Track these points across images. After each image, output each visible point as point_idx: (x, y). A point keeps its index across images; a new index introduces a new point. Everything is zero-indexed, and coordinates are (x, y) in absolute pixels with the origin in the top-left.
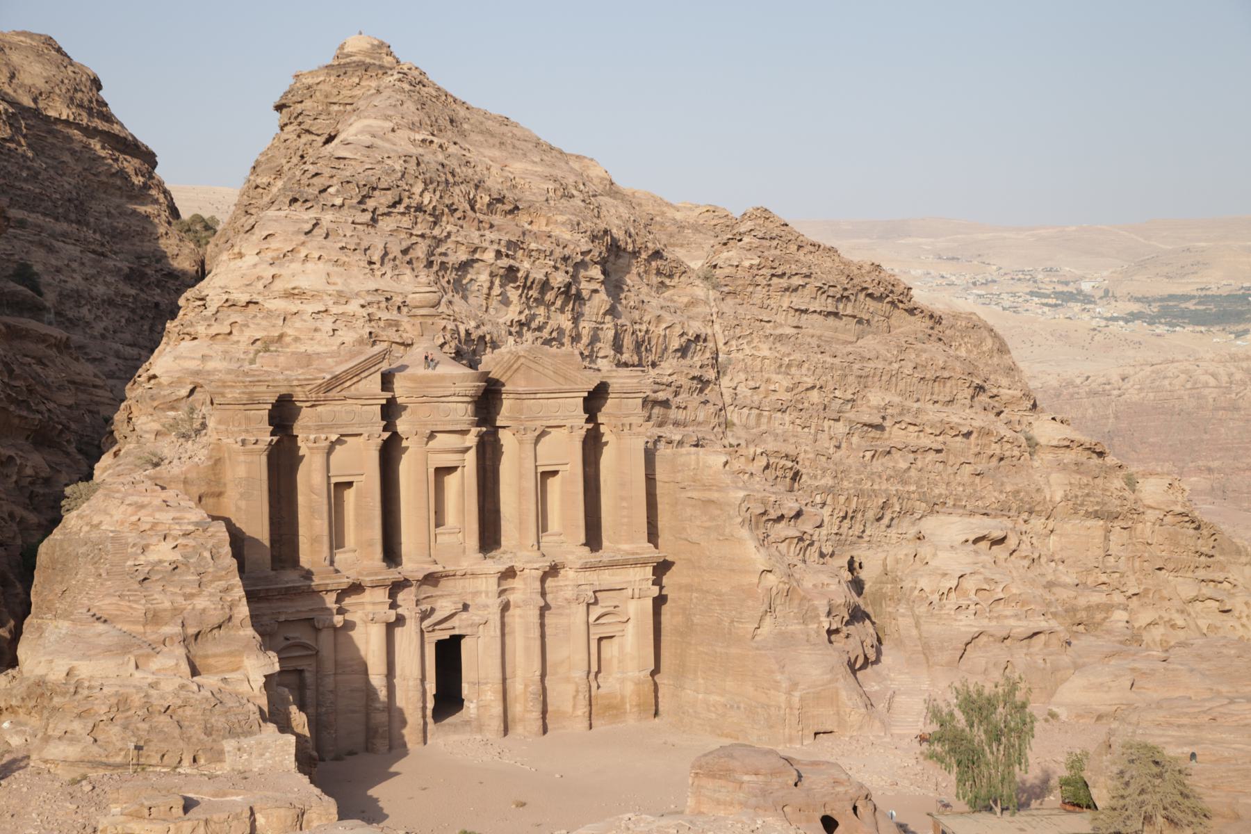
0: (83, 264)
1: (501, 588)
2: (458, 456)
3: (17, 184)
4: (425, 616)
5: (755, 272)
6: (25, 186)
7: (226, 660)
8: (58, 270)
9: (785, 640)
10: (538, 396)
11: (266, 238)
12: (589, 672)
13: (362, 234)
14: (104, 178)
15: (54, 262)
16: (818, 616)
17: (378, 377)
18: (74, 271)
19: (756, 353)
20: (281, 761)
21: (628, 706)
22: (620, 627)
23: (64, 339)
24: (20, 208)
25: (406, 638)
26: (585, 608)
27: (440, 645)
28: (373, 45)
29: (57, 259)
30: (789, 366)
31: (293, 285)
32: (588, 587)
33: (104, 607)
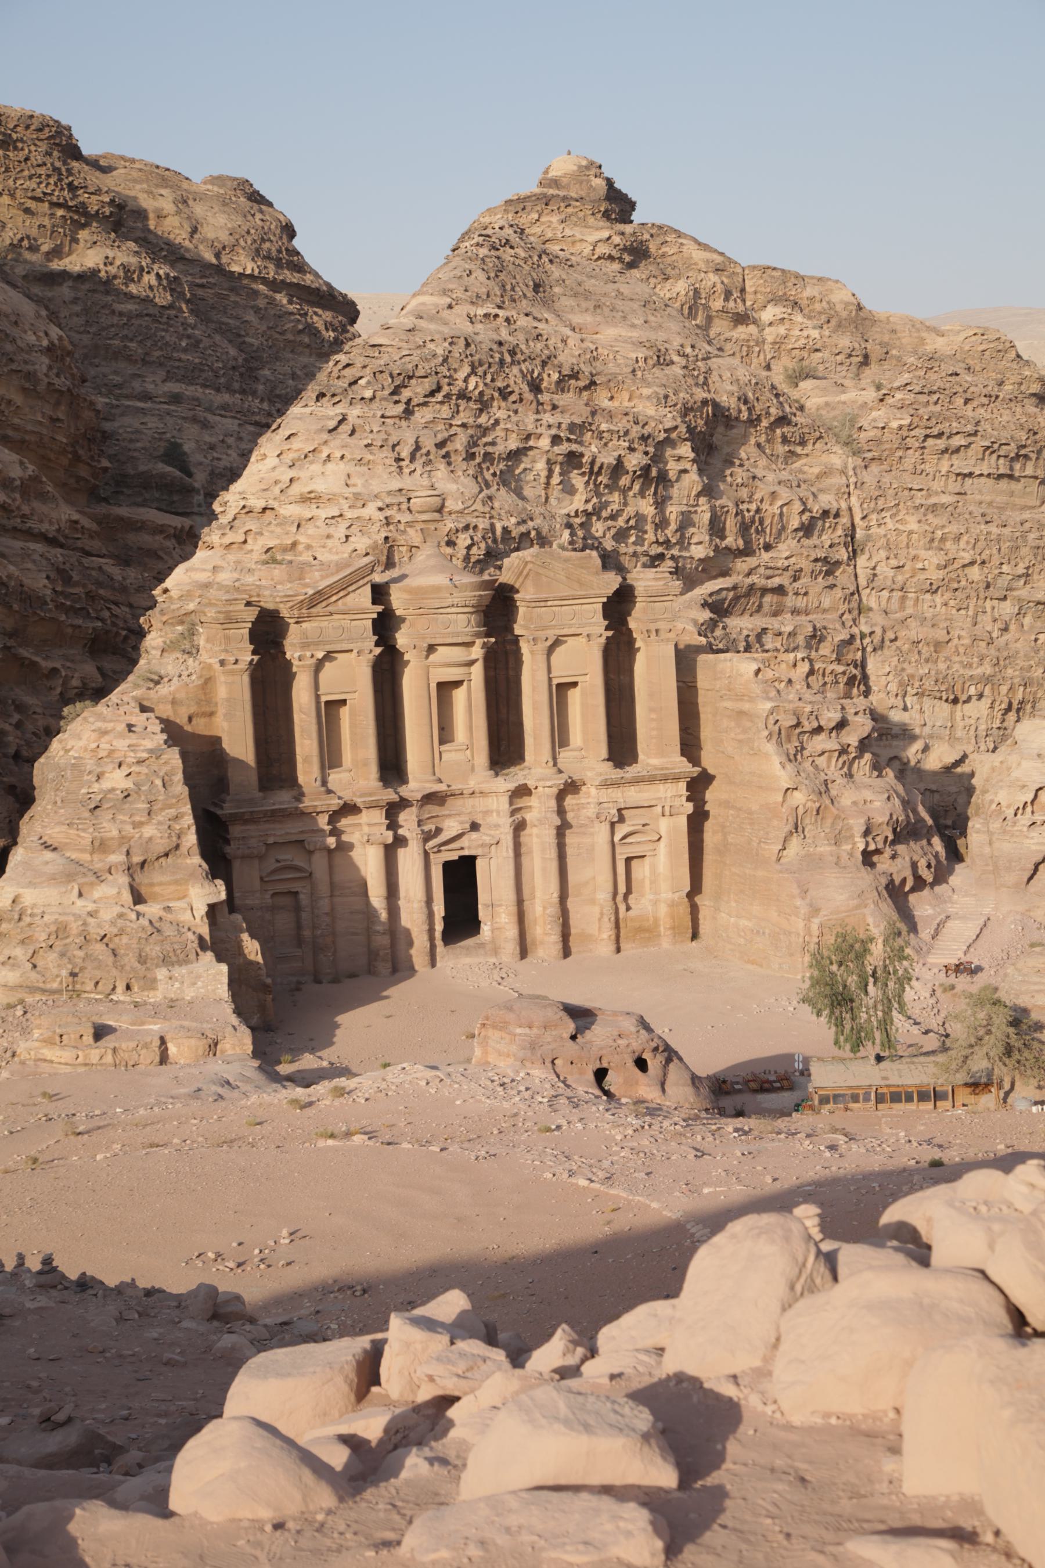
0: (240, 439)
1: (514, 807)
2: (462, 670)
3: (175, 355)
4: (427, 837)
5: (905, 433)
6: (183, 356)
7: (172, 888)
8: (212, 447)
9: (812, 862)
10: (549, 603)
11: (289, 438)
12: (615, 893)
13: (390, 429)
14: (290, 337)
15: (207, 439)
16: (852, 836)
17: (368, 589)
18: (229, 447)
19: (901, 527)
20: (214, 990)
21: (662, 929)
22: (651, 846)
23: (187, 528)
24: (178, 381)
25: (409, 861)
26: (608, 827)
27: (448, 867)
28: (580, 167)
29: (211, 435)
30: (943, 539)
31: (309, 489)
32: (611, 805)
33: (54, 835)
